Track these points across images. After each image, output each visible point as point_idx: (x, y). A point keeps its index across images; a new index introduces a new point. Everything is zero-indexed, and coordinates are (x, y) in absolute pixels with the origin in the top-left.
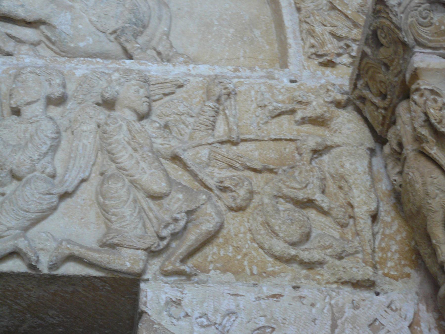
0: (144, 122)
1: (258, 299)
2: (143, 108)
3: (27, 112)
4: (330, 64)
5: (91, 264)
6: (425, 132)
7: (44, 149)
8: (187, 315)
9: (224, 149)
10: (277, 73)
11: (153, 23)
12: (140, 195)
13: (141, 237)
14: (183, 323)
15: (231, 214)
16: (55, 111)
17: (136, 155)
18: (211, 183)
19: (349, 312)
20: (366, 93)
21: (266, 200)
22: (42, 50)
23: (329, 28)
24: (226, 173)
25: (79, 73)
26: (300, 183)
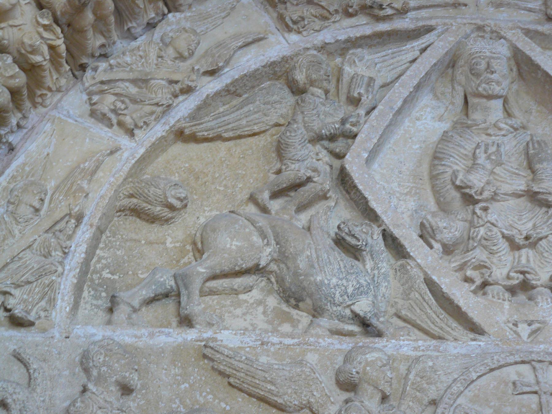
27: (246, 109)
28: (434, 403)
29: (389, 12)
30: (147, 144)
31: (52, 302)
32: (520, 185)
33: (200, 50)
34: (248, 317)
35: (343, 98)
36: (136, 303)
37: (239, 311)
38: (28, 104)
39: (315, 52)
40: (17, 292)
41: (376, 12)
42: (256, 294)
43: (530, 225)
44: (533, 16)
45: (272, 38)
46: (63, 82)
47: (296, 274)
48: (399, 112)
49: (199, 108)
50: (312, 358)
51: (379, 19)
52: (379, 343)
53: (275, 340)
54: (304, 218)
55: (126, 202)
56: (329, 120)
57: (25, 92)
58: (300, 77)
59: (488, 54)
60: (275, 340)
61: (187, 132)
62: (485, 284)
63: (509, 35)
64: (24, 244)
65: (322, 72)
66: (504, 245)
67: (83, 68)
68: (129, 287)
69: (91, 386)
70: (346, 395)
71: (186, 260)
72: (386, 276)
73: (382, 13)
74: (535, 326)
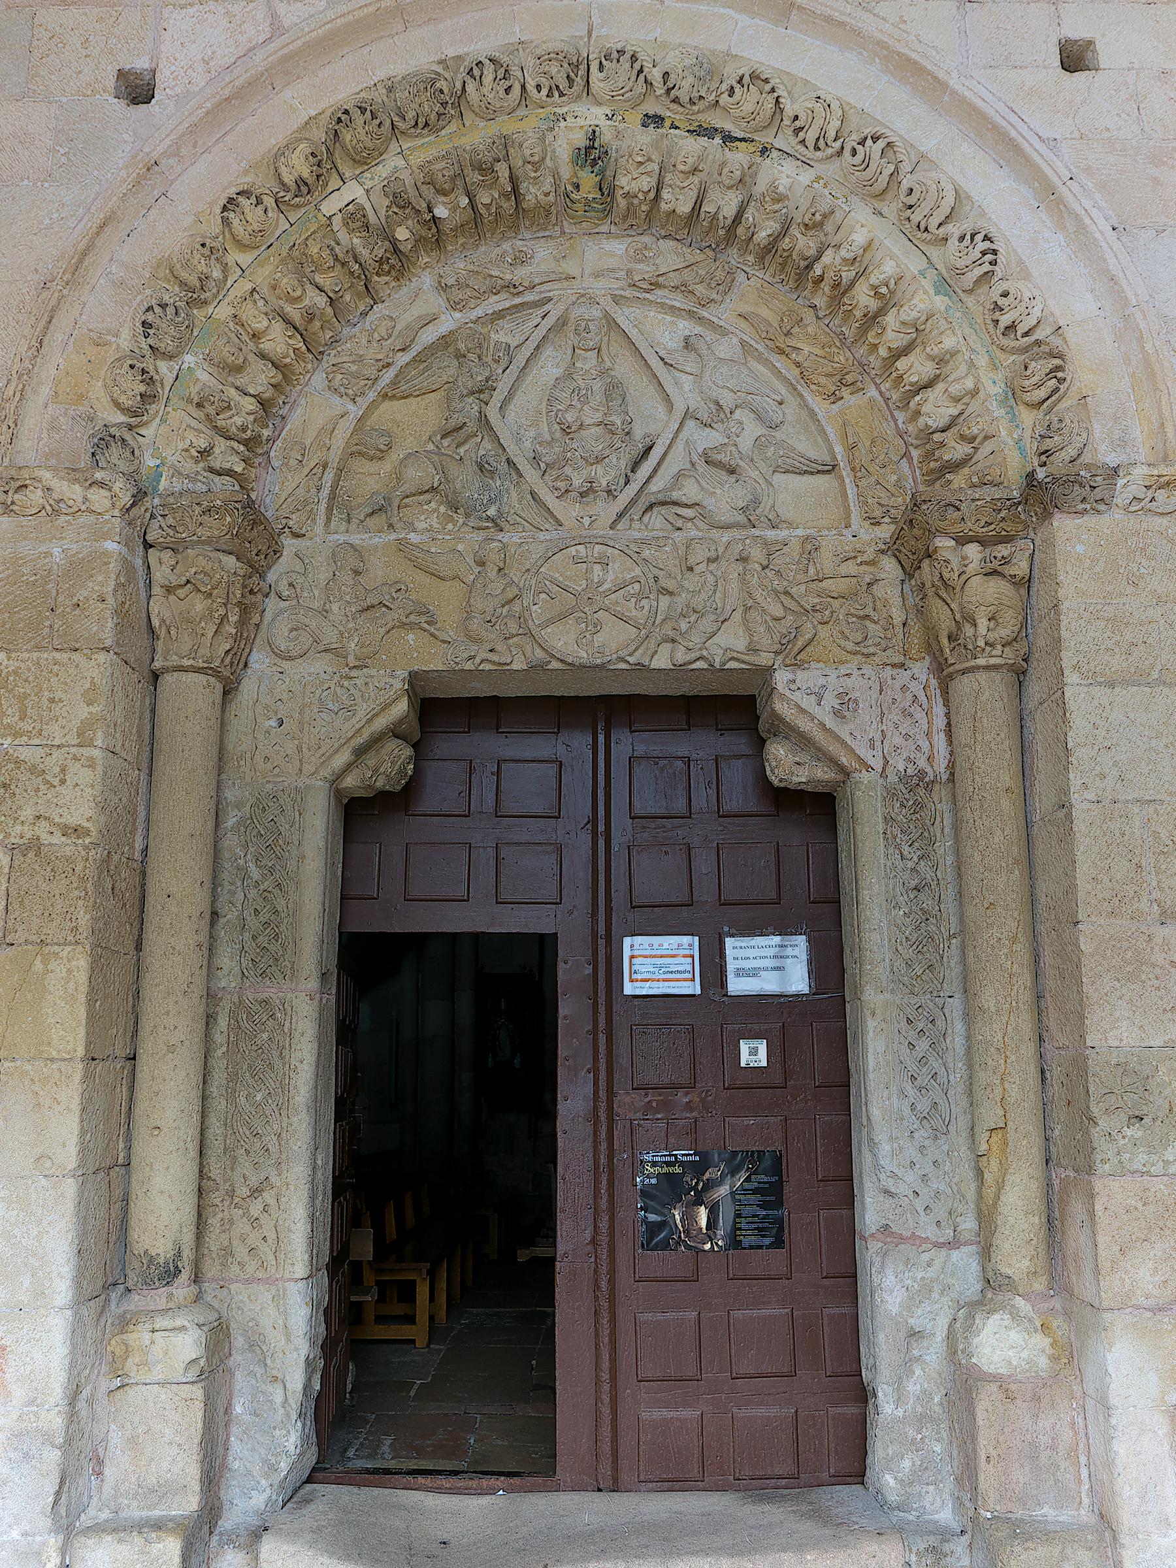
0: (766, 571)
1: (838, 677)
2: (765, 563)
3: (698, 569)
4: (879, 523)
5: (743, 662)
6: (940, 584)
7: (711, 592)
8: (799, 689)
9: (814, 585)
10: (845, 532)
11: (765, 499)
12: (768, 618)
13: (771, 645)
14: (798, 693)
15: (820, 626)
16: (713, 566)
17: (764, 593)
18: (809, 607)
19: (890, 682)
20: (902, 548)
21: (841, 617)
22: (700, 524)
23: (876, 500)
24: (817, 600)
25: (724, 539)
26: (861, 605)
27: (426, 374)
28: (528, 570)
29: (521, 289)
30: (364, 407)
31: (314, 520)
32: (598, 417)
33: (396, 333)
34: (428, 521)
35: (490, 358)
36: (362, 518)
37: (423, 518)
38: (288, 388)
39: (472, 325)
40: (294, 516)
41: (512, 290)
42: (433, 504)
43: (600, 447)
44: (619, 284)
45: (443, 317)
46: (309, 366)
47: (454, 492)
48: (524, 368)
49: (397, 376)
50: (460, 547)
51: (514, 295)
52: (500, 536)
53: (440, 537)
54: (462, 450)
55: (354, 449)
56: (479, 378)
57: (283, 383)
58: (462, 346)
59: (587, 317)
60: (440, 537)
61: (389, 394)
62: (567, 491)
63: (602, 301)
64: (294, 485)
65: (476, 340)
66: (581, 463)
67: (322, 353)
68: (360, 505)
69: (337, 573)
70: (480, 569)
71: (392, 484)
72: (507, 490)
73: (515, 291)
74: (594, 517)
